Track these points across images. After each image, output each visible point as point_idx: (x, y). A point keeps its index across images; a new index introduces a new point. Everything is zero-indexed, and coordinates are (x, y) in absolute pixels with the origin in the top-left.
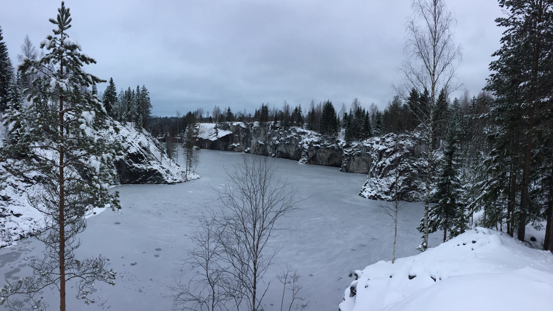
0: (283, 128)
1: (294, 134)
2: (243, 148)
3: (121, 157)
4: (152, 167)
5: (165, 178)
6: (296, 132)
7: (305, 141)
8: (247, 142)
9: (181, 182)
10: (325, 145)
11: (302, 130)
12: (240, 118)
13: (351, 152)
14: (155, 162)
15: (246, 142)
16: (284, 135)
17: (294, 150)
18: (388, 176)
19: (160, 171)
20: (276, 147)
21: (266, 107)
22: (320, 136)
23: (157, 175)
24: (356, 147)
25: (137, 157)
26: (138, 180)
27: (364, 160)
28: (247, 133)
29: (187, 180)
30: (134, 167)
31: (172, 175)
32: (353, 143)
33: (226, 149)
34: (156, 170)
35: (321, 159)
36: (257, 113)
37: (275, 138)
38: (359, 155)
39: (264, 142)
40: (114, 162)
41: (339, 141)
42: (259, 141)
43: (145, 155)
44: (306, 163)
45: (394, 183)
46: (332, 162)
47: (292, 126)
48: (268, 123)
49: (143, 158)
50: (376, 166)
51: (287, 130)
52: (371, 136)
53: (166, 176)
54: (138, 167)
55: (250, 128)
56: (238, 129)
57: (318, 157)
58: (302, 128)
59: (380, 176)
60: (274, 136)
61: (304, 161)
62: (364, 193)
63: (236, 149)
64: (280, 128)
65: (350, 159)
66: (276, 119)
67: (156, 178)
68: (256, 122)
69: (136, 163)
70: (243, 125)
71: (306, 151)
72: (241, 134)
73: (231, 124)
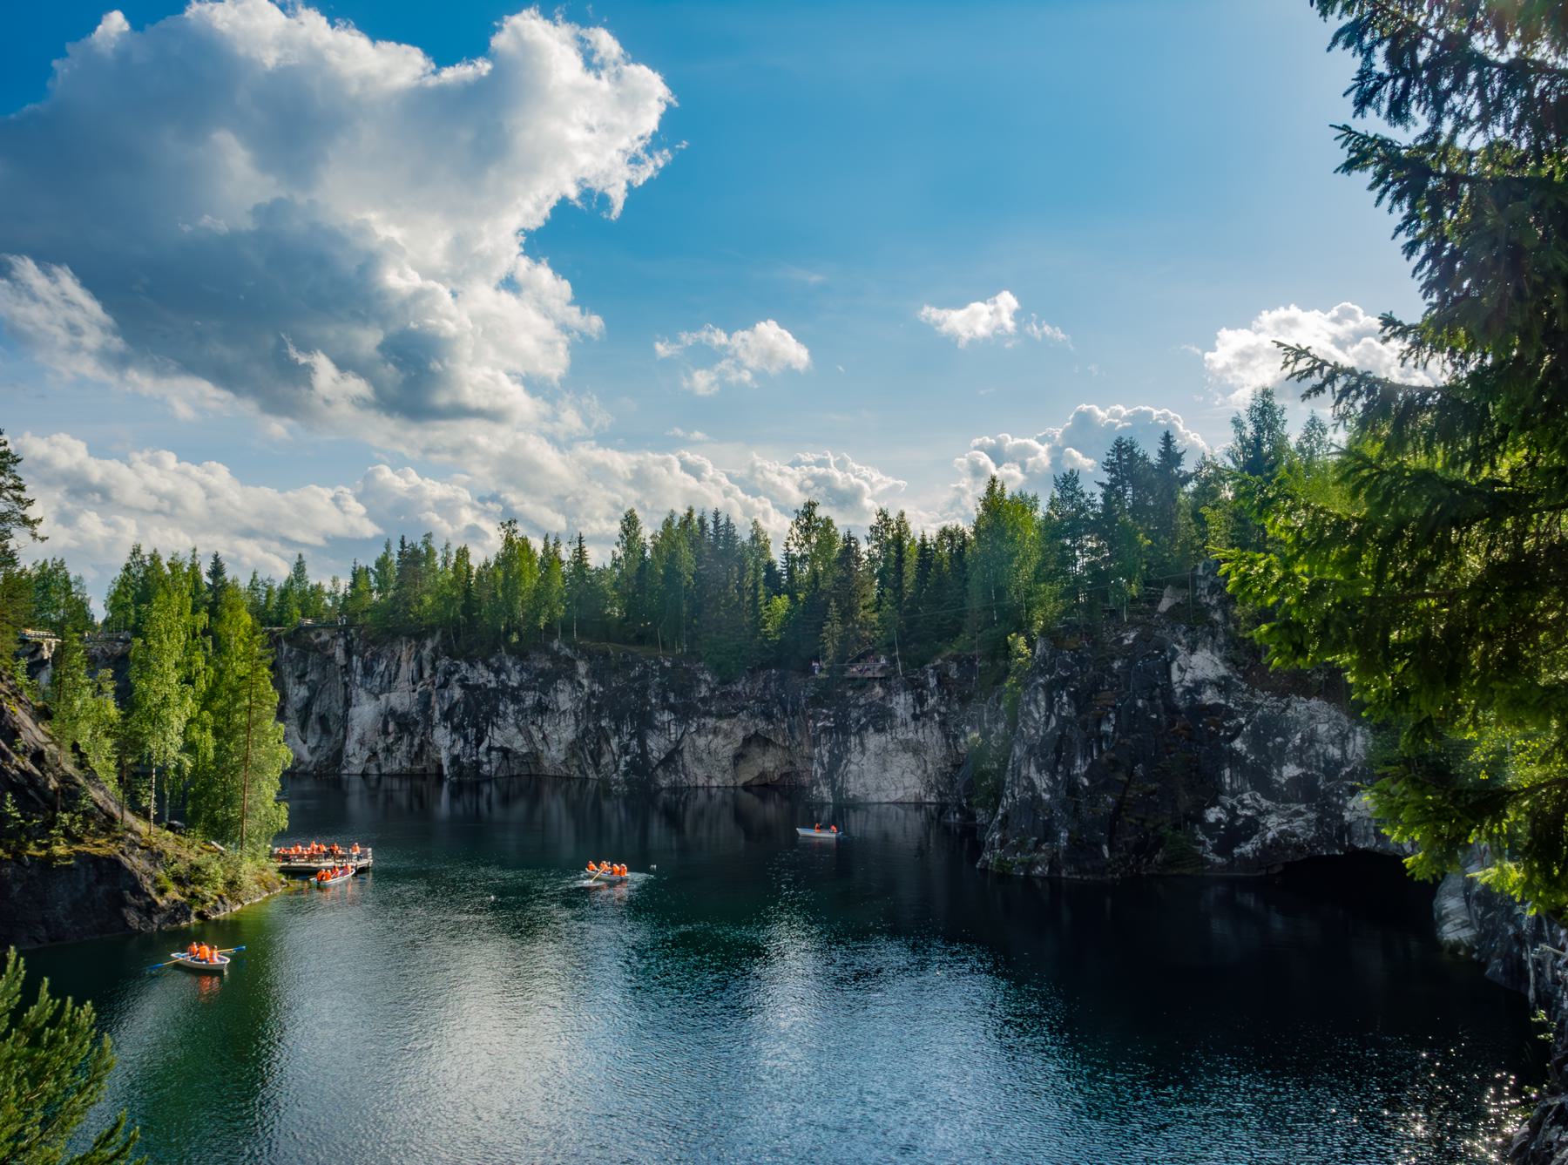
27: (906, 746)
35: (700, 760)
57: (687, 756)
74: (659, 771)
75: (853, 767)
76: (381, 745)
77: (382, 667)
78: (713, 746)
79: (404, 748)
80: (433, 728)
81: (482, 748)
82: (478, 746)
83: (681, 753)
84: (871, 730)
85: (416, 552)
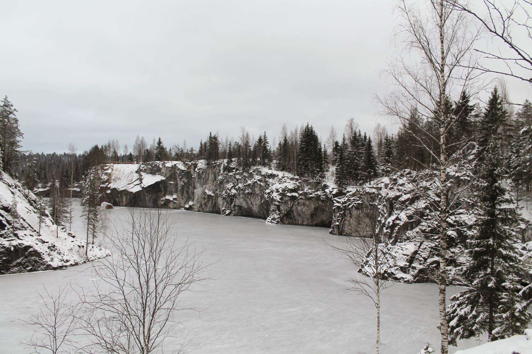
0: (241, 168)
1: (257, 177)
2: (182, 202)
4: (20, 242)
5: (47, 259)
6: (261, 175)
7: (274, 188)
8: (187, 192)
9: (77, 264)
10: (305, 194)
11: (270, 172)
13: (345, 202)
15: (187, 192)
16: (243, 181)
17: (258, 202)
18: (405, 240)
19: (37, 248)
20: (231, 198)
21: (215, 138)
22: (297, 180)
23: (32, 255)
24: (353, 195)
27: (367, 215)
28: (187, 178)
31: (60, 254)
32: (349, 189)
33: (156, 205)
34: (30, 247)
35: (300, 215)
36: (203, 148)
37: (230, 185)
38: (359, 207)
39: (214, 192)
41: (326, 187)
42: (207, 191)
43: (8, 221)
44: (278, 222)
45: (416, 253)
46: (317, 220)
47: (254, 165)
48: (218, 162)
50: (384, 224)
51: (247, 172)
52: (376, 175)
55: (192, 170)
56: (175, 173)
57: (295, 214)
59: (391, 241)
60: (228, 182)
61: (274, 219)
62: (366, 268)
63: (171, 205)
64: (237, 170)
65: (344, 215)
66: (230, 155)
67: (29, 261)
68: (202, 161)
70: (181, 166)
71: (277, 203)
72: (178, 179)
73: (163, 164)
74: (285, 218)
75: (347, 222)
76: (203, 203)
78: (303, 210)
79: (210, 204)
81: (232, 205)
83: (293, 211)
84: (354, 208)
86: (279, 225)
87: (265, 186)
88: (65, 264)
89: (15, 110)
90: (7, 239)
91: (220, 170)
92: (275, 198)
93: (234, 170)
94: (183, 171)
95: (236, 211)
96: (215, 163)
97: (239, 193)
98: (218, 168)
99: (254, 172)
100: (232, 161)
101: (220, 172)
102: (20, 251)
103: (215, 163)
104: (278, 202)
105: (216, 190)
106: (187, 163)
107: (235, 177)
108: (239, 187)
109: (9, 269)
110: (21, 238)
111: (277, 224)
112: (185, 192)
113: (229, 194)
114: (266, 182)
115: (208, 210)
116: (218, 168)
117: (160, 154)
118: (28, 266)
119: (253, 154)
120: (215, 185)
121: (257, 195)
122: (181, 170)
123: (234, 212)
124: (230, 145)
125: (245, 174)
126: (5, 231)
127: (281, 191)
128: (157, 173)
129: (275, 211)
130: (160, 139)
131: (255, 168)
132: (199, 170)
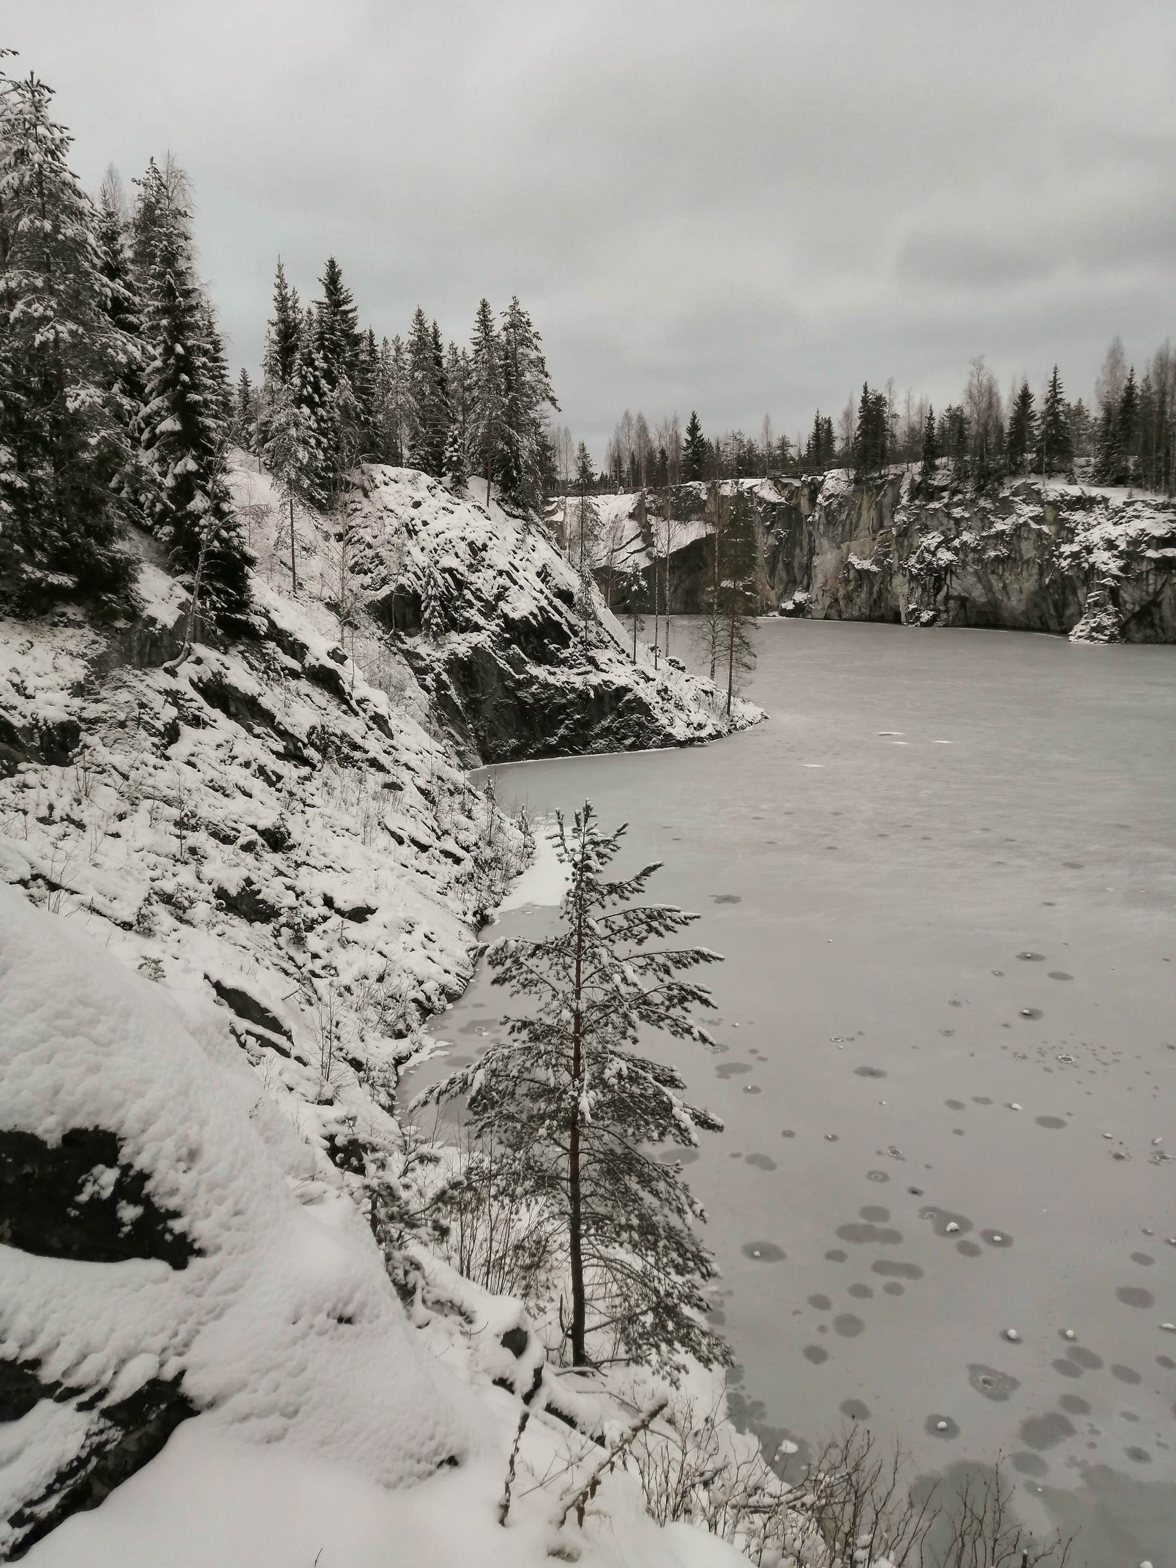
0: (969, 487)
2: (773, 595)
3: (475, 638)
4: (606, 677)
5: (663, 720)
6: (1042, 503)
7: (1095, 536)
8: (788, 566)
9: (719, 735)
11: (1074, 491)
12: (740, 460)
14: (611, 653)
16: (976, 523)
17: (1029, 583)
19: (642, 695)
20: (938, 576)
23: (633, 710)
25: (539, 637)
26: (553, 741)
28: (787, 526)
29: (733, 729)
30: (533, 680)
36: (823, 434)
37: (932, 539)
39: (877, 562)
40: (448, 662)
42: (853, 559)
43: (571, 627)
44: (1112, 638)
47: (1014, 474)
48: (892, 470)
49: (564, 641)
51: (992, 496)
53: (664, 711)
54: (551, 680)
55: (804, 503)
56: (748, 512)
58: (1072, 482)
60: (925, 530)
61: (1099, 629)
64: (955, 492)
68: (835, 472)
69: (540, 662)
70: (767, 491)
72: (759, 531)
73: (713, 491)
76: (841, 592)
77: (844, 516)
79: (863, 595)
80: (891, 576)
81: (940, 597)
82: (936, 595)
85: (879, 399)
86: (1115, 645)
87: (1057, 535)
88: (697, 734)
89: (536, 335)
90: (575, 670)
91: (897, 499)
92: (1104, 568)
93: (945, 494)
94: (774, 506)
95: (951, 613)
96: (881, 477)
97: (964, 561)
98: (889, 492)
99: (1014, 494)
100: (935, 468)
101: (898, 502)
102: (607, 699)
103: (881, 477)
104: (1114, 577)
105: (886, 555)
106: (785, 481)
107: (948, 515)
108: (964, 544)
109: (588, 743)
110: (603, 666)
111: (1108, 642)
112: (780, 565)
113: (930, 563)
114: (1061, 523)
115: (856, 613)
116: (889, 492)
117: (698, 461)
118: (625, 737)
119: (1001, 446)
120: (882, 542)
121: (1027, 562)
122: (769, 503)
123: (944, 616)
124: (931, 418)
125: (983, 503)
126: (570, 650)
127: (1123, 546)
128: (694, 516)
129: (1102, 605)
130: (695, 417)
131: (1018, 482)
132: (828, 498)
